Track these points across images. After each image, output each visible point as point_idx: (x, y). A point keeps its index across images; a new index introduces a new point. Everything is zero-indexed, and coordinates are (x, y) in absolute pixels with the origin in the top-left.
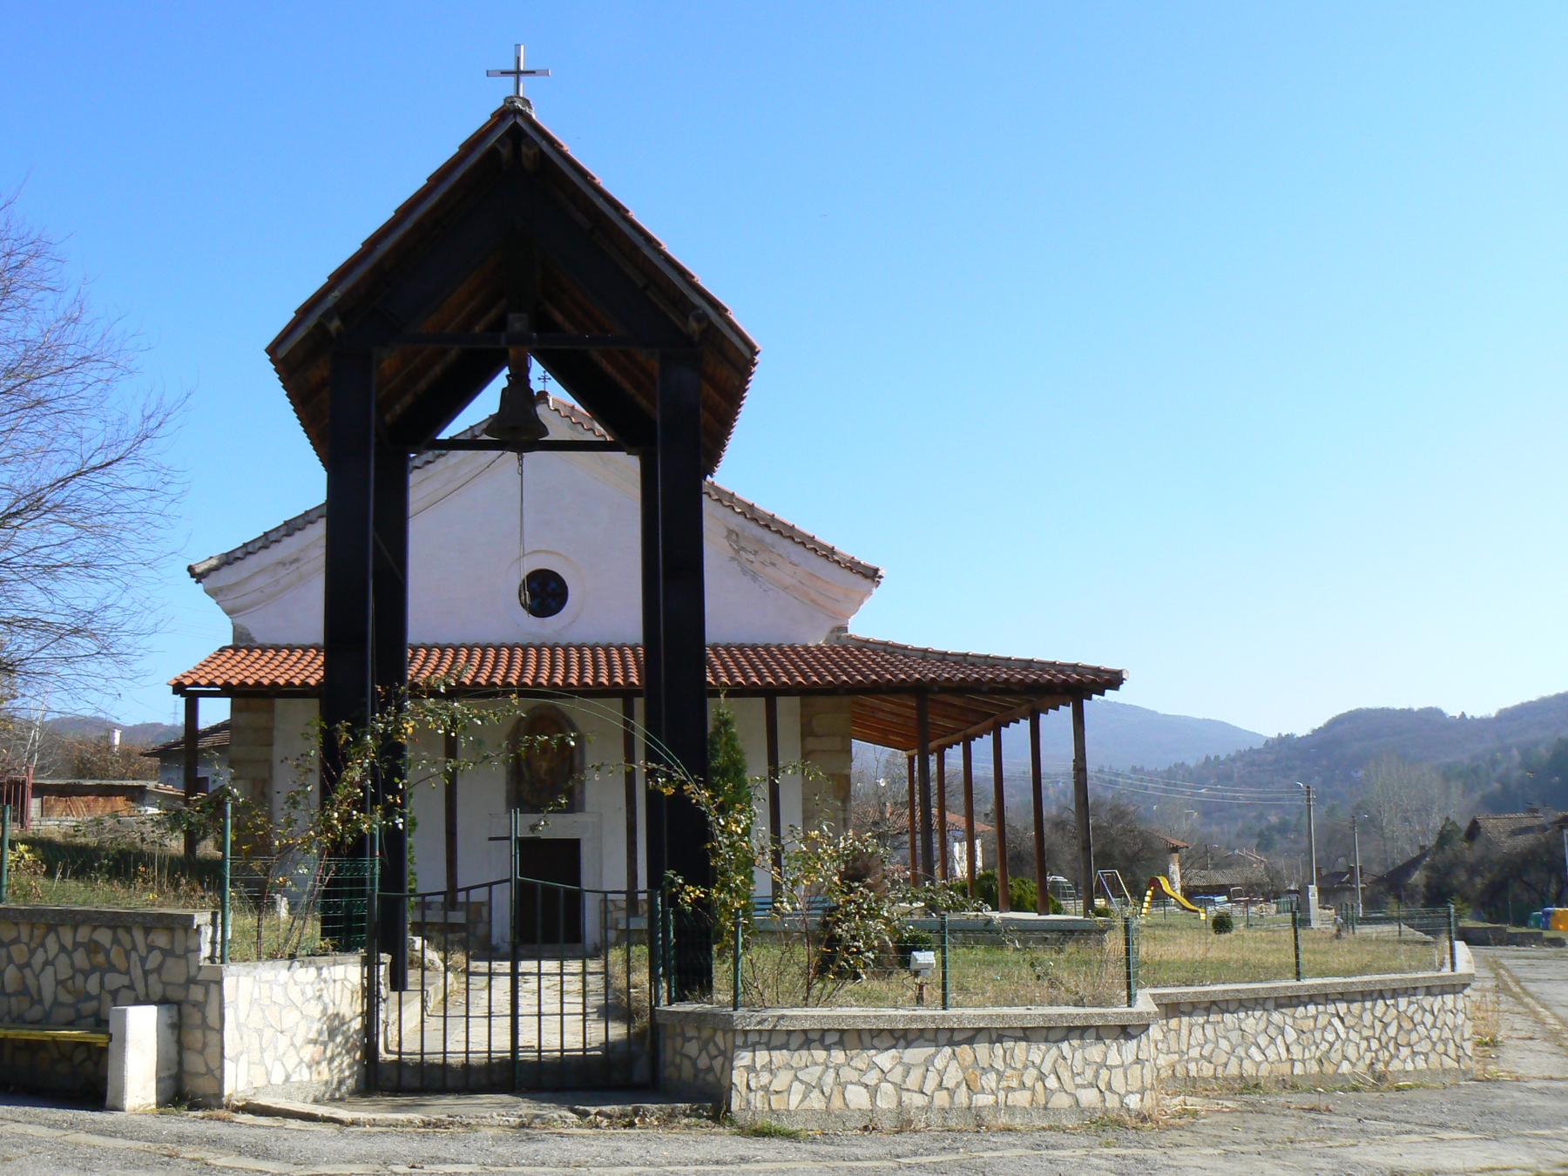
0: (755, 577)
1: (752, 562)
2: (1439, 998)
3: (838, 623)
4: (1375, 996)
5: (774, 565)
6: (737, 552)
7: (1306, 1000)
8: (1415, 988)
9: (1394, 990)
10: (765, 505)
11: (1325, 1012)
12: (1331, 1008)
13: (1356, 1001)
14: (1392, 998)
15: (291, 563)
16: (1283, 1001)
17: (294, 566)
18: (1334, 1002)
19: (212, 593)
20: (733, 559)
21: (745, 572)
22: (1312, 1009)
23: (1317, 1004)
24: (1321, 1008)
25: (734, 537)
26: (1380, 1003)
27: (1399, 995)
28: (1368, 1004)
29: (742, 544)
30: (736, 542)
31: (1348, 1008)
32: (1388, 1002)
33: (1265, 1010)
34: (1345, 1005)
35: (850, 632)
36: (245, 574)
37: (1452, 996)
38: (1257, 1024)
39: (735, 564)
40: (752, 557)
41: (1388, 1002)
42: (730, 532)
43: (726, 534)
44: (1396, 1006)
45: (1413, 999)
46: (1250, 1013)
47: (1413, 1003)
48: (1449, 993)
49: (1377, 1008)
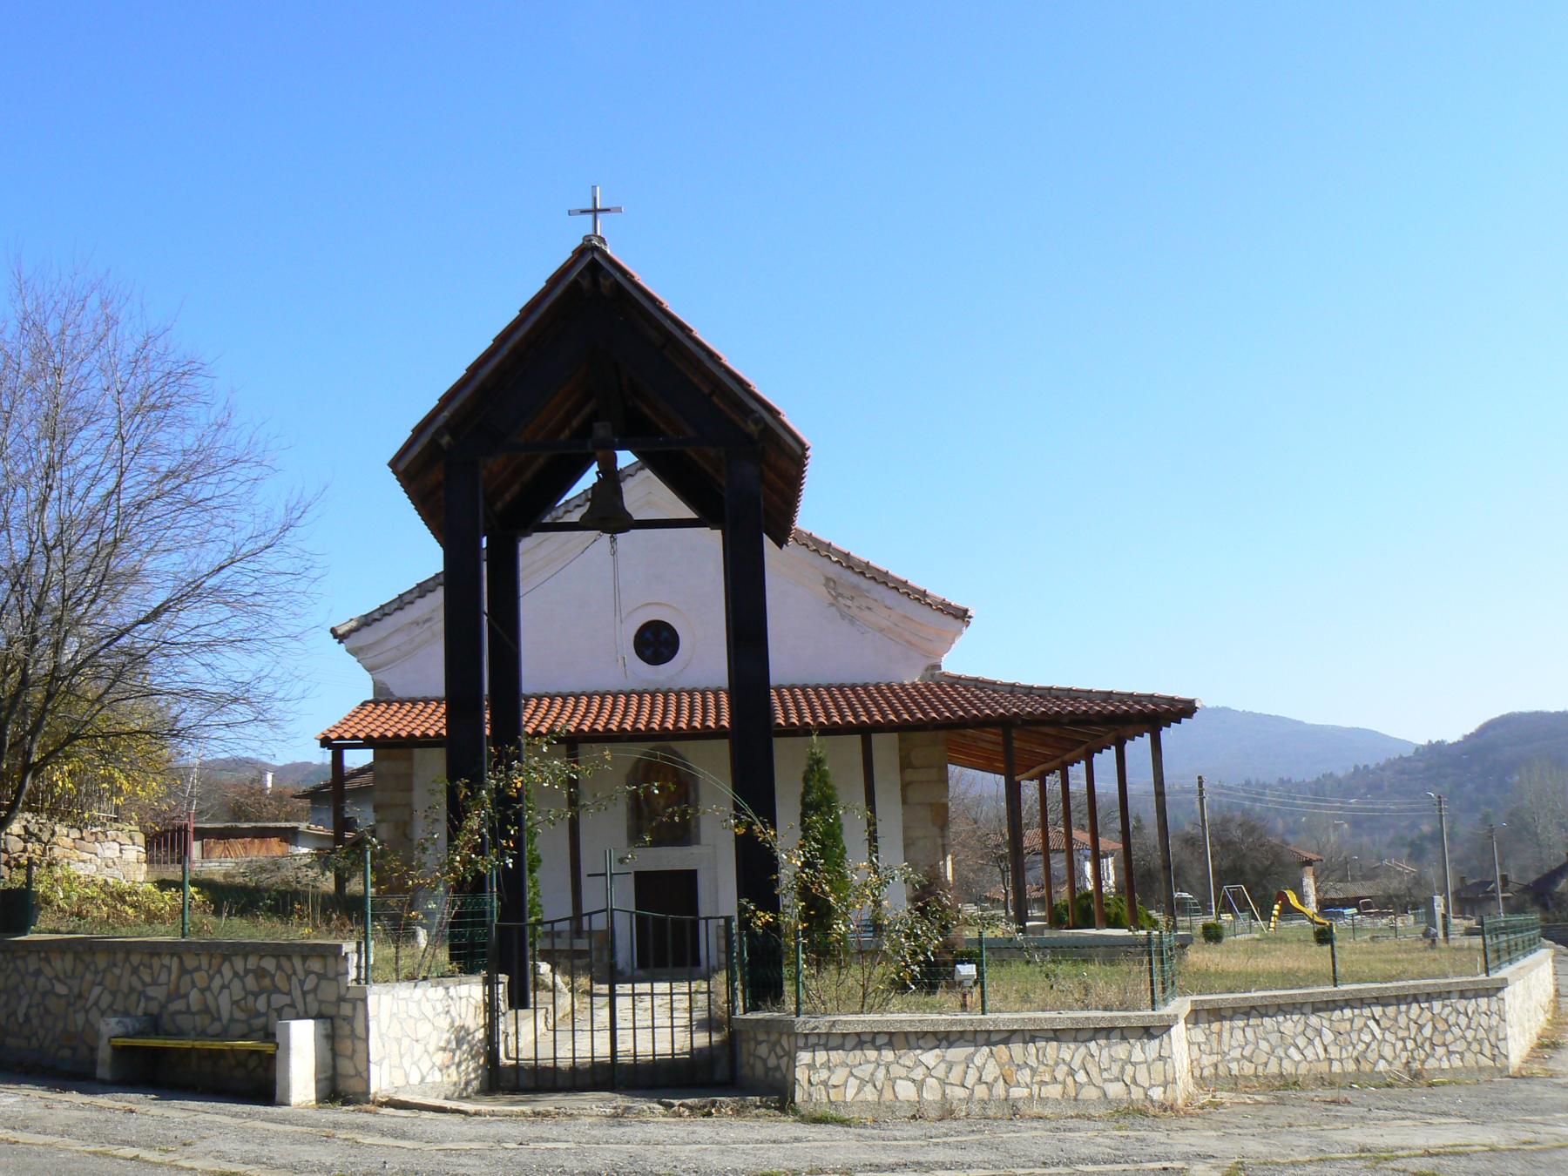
0: (852, 621)
1: (849, 607)
2: (1473, 1000)
3: (933, 662)
4: (1409, 1000)
5: (869, 609)
6: (835, 598)
7: (1342, 1004)
8: (1449, 992)
9: (1428, 994)
10: (860, 553)
11: (1361, 1015)
12: (1367, 1012)
13: (1391, 1005)
14: (1427, 1001)
15: (425, 622)
16: (1320, 1006)
17: (428, 624)
18: (1369, 1005)
19: (353, 652)
20: (832, 605)
21: (843, 617)
22: (1348, 1013)
23: (1352, 1008)
24: (1357, 1011)
25: (832, 584)
26: (1415, 1006)
27: (1433, 999)
28: (1403, 1008)
29: (840, 590)
30: (834, 589)
31: (1384, 1011)
32: (1422, 1005)
33: (1302, 1014)
34: (1380, 1008)
35: (943, 670)
36: (383, 634)
37: (1486, 999)
38: (1295, 1026)
39: (834, 609)
40: (849, 603)
41: (1422, 1005)
42: (828, 579)
43: (824, 582)
44: (1430, 1009)
45: (1447, 1002)
46: (1288, 1017)
47: (1447, 1006)
48: (1483, 996)
49: (1412, 1011)
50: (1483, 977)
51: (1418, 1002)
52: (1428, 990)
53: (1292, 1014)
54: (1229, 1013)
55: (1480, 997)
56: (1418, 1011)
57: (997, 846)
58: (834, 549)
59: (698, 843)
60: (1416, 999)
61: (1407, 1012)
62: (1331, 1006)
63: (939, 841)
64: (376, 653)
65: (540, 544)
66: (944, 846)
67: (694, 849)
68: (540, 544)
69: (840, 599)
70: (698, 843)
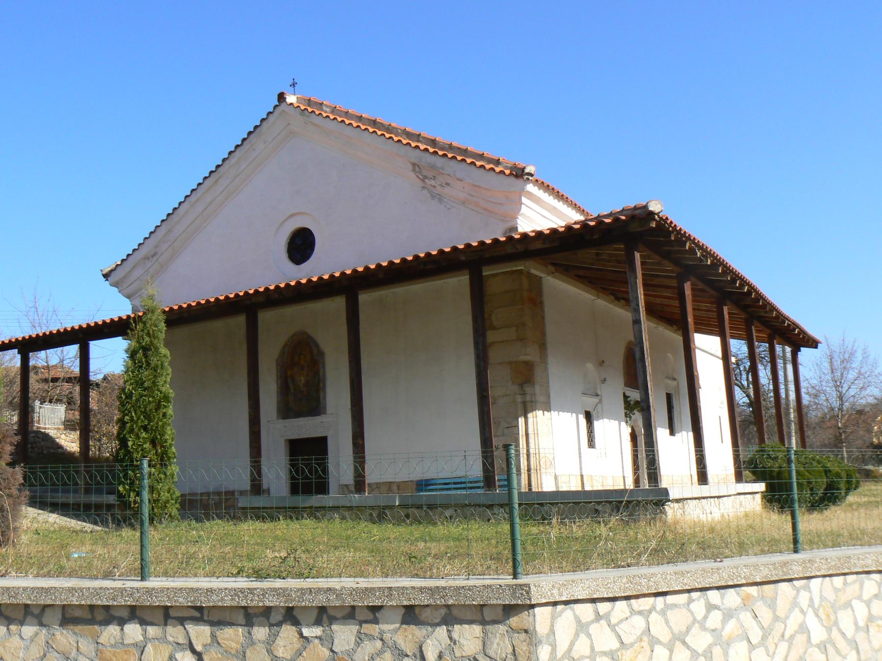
0: (440, 198)
1: (435, 187)
2: (442, 631)
3: (509, 225)
4: (276, 617)
5: (448, 184)
6: (423, 181)
7: (125, 614)
8: (375, 609)
9: (322, 610)
10: (442, 137)
11: (163, 640)
12: (175, 633)
13: (231, 624)
14: (318, 622)
15: (153, 256)
16: (78, 613)
17: (155, 258)
18: (182, 621)
19: (115, 285)
20: (424, 188)
21: (433, 197)
22: (133, 631)
23: (143, 622)
24: (152, 630)
25: (417, 169)
26: (288, 632)
27: (332, 620)
28: (260, 632)
29: (425, 173)
30: (420, 172)
31: (213, 636)
32: (306, 632)
33: (41, 624)
34: (206, 630)
35: (520, 230)
36: (127, 270)
37: (477, 629)
38: (27, 648)
39: (425, 192)
40: (433, 182)
41: (306, 632)
42: (414, 165)
43: (411, 168)
44: (327, 640)
45: (368, 628)
46: (13, 628)
47: (371, 637)
48: (471, 622)
49: (280, 642)
50: (508, 580)
51: (296, 623)
52: (321, 600)
53: (22, 623)
54: (125, 614)
55: (461, 622)
56: (297, 644)
57: (116, 384)
58: (424, 138)
59: (325, 413)
60: (291, 616)
61: (270, 643)
62: (100, 616)
63: (519, 399)
64: (128, 284)
65: (216, 182)
66: (524, 403)
67: (318, 420)
68: (216, 182)
69: (426, 180)
70: (325, 413)
